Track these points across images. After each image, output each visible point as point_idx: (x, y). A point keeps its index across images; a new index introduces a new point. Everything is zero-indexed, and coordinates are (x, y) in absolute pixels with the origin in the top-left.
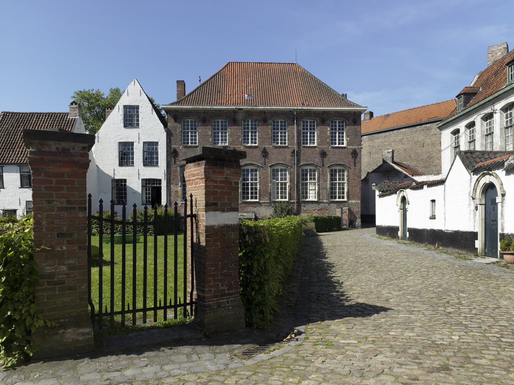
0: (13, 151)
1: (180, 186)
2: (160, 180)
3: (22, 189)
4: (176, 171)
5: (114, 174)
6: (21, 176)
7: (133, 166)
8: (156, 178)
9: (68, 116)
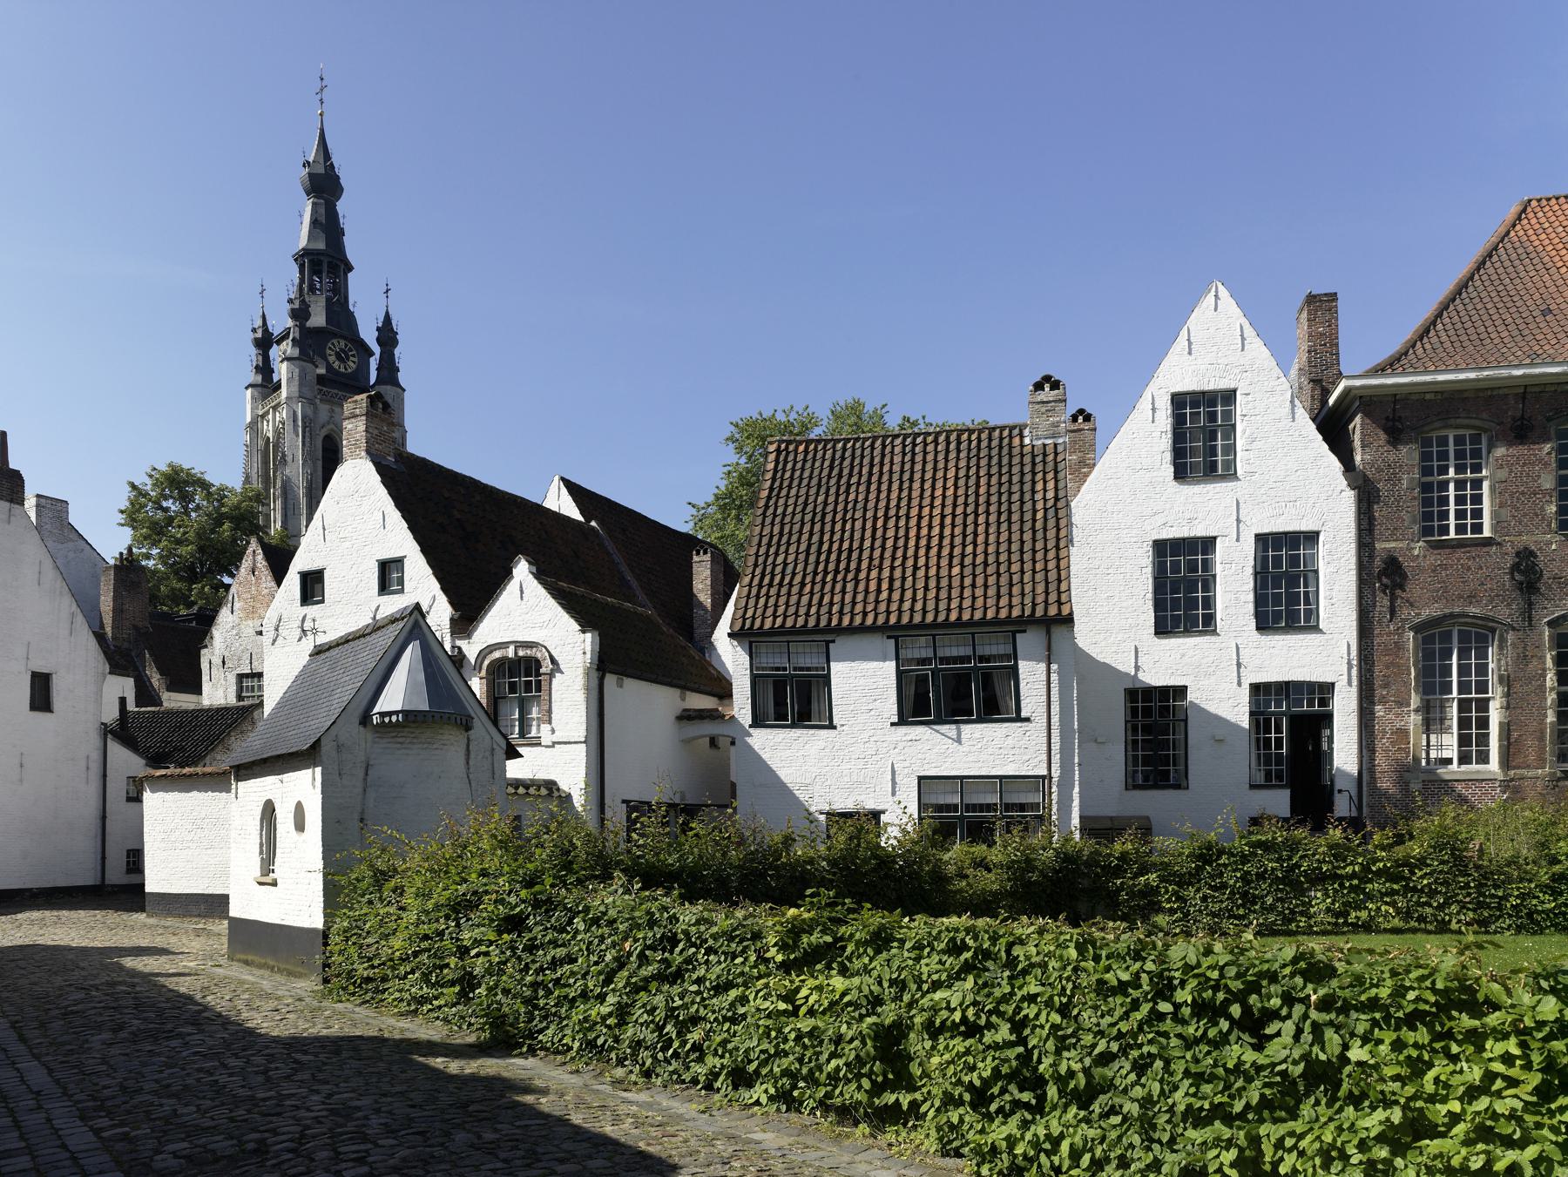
0: (857, 581)
1: (1417, 711)
2: (1324, 691)
3: (903, 730)
4: (1399, 647)
5: (1137, 668)
6: (900, 674)
7: (1214, 632)
8: (1313, 679)
9: (1022, 437)
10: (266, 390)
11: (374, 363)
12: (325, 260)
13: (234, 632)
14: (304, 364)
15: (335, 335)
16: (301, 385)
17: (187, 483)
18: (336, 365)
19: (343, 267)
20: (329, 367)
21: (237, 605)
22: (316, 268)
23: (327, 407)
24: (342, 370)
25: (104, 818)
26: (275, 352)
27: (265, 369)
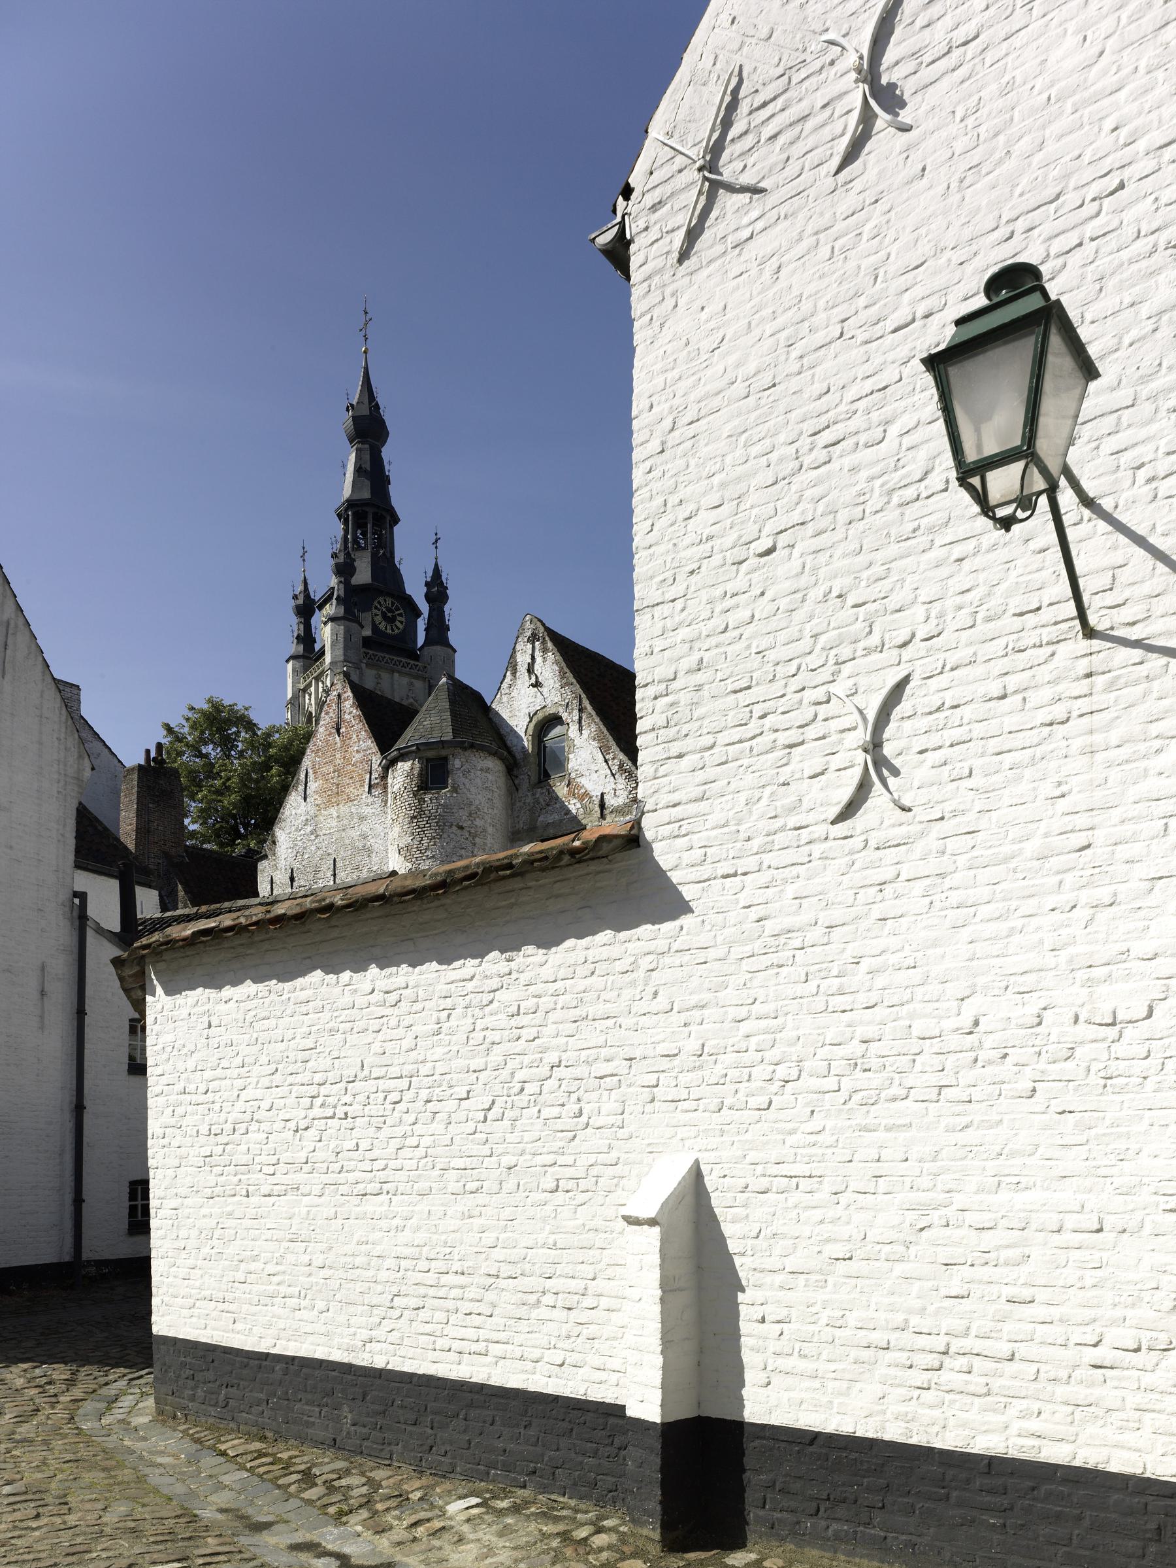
10: (308, 661)
11: (421, 624)
12: (370, 511)
13: (309, 829)
14: (348, 623)
15: (381, 593)
16: (346, 648)
17: (229, 722)
18: (382, 626)
19: (388, 518)
20: (375, 628)
21: (313, 786)
22: (360, 523)
23: (374, 672)
24: (389, 631)
25: (79, 1108)
26: (318, 618)
27: (307, 639)
